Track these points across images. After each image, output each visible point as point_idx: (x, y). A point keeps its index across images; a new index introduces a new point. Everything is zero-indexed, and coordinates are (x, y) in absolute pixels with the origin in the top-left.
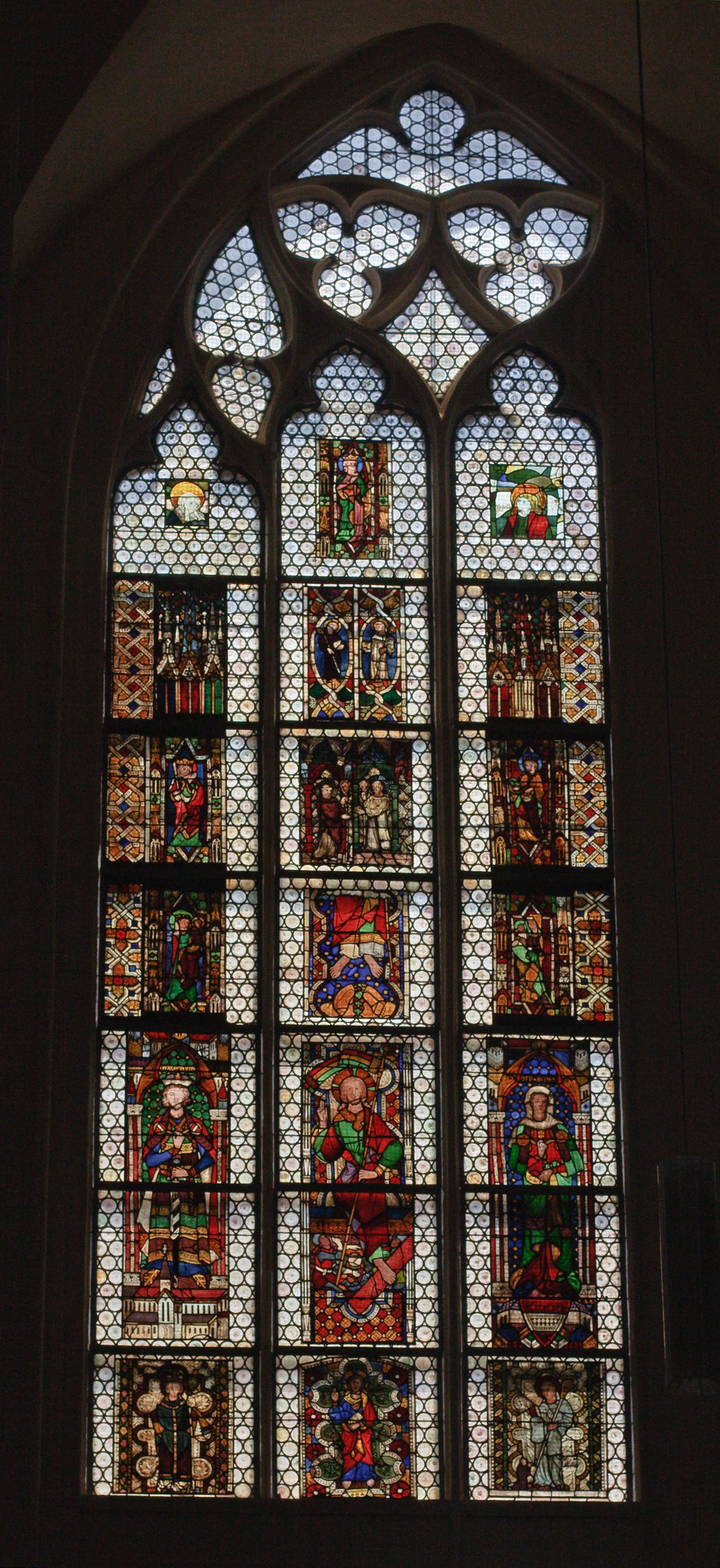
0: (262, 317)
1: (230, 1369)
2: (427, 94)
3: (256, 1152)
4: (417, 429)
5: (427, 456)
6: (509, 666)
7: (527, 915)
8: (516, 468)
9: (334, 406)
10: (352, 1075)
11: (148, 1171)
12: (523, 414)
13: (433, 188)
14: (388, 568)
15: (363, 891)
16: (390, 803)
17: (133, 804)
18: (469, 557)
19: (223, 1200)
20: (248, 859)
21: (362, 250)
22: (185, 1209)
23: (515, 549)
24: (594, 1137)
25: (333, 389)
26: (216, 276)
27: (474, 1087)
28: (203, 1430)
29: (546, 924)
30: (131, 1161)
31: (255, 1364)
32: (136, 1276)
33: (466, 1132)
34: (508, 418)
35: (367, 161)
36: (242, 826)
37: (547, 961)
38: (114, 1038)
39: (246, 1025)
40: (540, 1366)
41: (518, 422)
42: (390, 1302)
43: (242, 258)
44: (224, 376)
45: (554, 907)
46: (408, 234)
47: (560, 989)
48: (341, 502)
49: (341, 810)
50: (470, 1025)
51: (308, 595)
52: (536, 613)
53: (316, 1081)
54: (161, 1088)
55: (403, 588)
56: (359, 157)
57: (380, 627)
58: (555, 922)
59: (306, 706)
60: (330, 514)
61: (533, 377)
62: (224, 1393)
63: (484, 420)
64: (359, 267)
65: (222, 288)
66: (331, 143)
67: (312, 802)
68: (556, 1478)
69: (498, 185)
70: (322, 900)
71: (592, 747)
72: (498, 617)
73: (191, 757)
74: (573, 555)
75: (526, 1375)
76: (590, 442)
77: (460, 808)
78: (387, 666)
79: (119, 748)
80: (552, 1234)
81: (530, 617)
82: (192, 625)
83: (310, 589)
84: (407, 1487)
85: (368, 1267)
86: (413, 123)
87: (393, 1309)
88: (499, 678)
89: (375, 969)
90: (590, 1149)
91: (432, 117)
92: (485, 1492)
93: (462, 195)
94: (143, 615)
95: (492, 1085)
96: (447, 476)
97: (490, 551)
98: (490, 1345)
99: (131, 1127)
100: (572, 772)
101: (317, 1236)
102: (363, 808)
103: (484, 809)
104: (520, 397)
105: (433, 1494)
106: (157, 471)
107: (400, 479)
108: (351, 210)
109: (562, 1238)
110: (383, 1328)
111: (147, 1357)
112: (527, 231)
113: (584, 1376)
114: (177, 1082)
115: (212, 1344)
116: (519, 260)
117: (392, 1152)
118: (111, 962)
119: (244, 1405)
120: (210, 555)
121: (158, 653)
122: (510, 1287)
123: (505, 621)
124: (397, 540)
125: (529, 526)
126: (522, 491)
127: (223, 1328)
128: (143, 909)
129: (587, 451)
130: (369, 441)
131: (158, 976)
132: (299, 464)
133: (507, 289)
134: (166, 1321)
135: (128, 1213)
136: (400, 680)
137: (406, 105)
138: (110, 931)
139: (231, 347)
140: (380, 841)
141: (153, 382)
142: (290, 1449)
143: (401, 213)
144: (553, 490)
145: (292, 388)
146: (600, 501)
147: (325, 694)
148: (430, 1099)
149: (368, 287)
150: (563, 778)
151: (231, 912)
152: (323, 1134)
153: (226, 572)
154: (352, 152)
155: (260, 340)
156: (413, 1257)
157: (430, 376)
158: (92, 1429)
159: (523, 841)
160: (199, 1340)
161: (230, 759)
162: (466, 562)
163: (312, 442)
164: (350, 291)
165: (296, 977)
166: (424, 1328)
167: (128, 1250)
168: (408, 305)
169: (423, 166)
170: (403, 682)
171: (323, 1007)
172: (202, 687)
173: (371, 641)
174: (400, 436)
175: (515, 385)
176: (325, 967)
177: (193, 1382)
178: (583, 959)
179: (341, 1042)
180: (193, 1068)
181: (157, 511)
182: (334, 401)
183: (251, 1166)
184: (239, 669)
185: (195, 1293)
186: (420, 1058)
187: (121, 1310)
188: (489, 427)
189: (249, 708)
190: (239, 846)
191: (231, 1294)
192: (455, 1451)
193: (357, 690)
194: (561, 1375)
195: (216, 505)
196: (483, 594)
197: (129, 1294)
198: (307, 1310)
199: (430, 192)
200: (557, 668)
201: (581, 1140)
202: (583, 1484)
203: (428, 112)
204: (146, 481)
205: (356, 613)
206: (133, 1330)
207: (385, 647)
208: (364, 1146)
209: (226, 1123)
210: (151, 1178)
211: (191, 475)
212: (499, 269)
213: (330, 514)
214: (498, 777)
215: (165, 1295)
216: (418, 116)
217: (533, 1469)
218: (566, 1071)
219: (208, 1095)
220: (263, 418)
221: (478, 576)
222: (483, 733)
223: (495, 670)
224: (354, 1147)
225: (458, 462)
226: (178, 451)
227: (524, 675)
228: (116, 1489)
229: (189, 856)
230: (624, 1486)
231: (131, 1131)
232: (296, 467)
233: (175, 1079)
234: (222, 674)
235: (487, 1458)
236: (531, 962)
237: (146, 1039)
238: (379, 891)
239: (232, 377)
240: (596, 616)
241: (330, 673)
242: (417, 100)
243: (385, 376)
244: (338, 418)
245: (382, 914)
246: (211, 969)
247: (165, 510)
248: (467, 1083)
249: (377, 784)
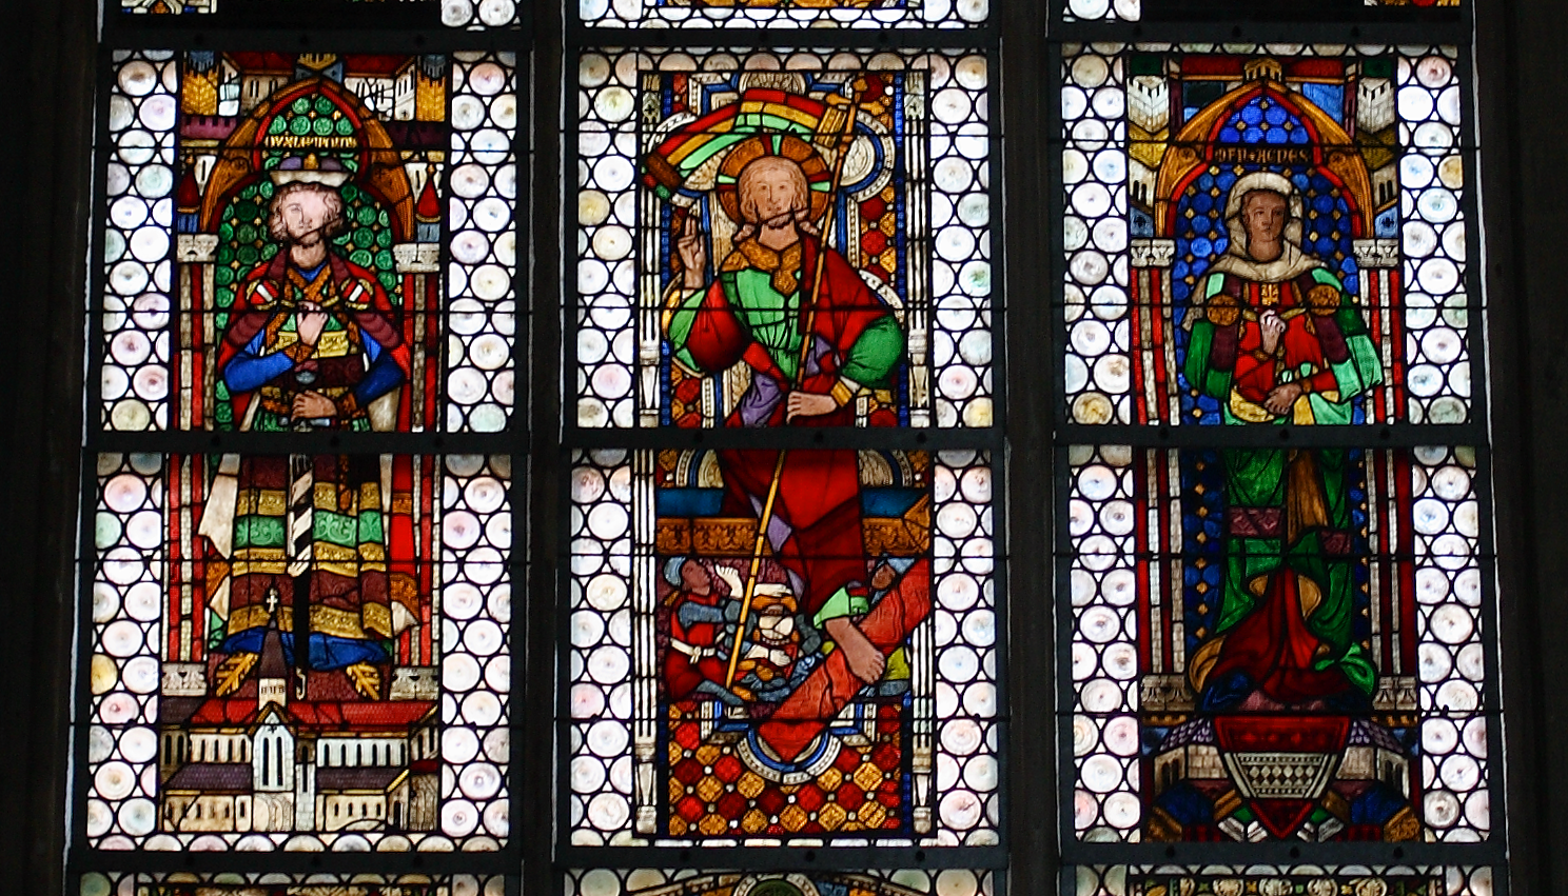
10: (769, 153)
11: (231, 403)
24: (1410, 300)
32: (195, 674)
33: (1071, 292)
42: (870, 728)
50: (1081, 22)
53: (676, 169)
80: (1300, 549)
85: (809, 639)
90: (1400, 331)
95: (1139, 173)
99: (186, 292)
101: (675, 563)
110: (851, 797)
111: (221, 878)
115: (398, 843)
122: (1189, 686)
127: (425, 802)
134: (273, 784)
148: (977, 209)
152: (696, 301)
160: (361, 833)
167: (175, 606)
180: (350, 141)
185: (349, 711)
187: (155, 760)
191: (448, 713)
197: (175, 718)
198: (647, 753)
201: (1375, 306)
206: (185, 810)
208: (801, 331)
210: (238, 419)
215: (273, 718)
219: (390, 207)
224: (776, 335)
231: (186, 303)
233: (302, 168)
248: (1074, 166)
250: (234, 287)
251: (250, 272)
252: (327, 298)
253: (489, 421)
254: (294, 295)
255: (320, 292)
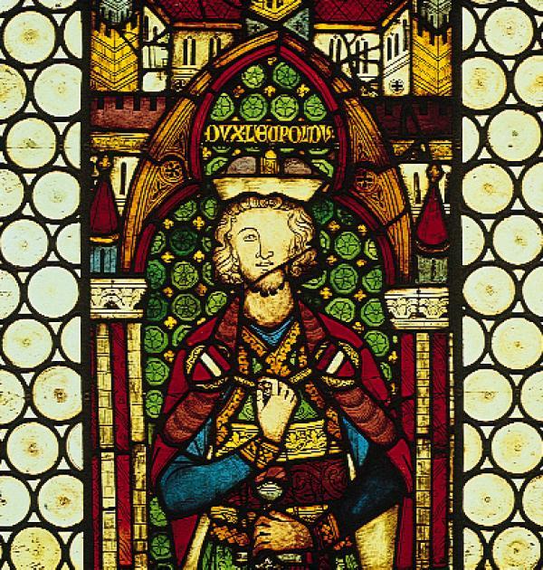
30: (109, 501)
114: (268, 186)
180: (324, 131)
209: (445, 341)
219: (379, 232)
231: (105, 382)
233: (258, 174)
250: (169, 355)
251: (191, 332)
252: (295, 369)
254: (250, 368)
255: (286, 363)
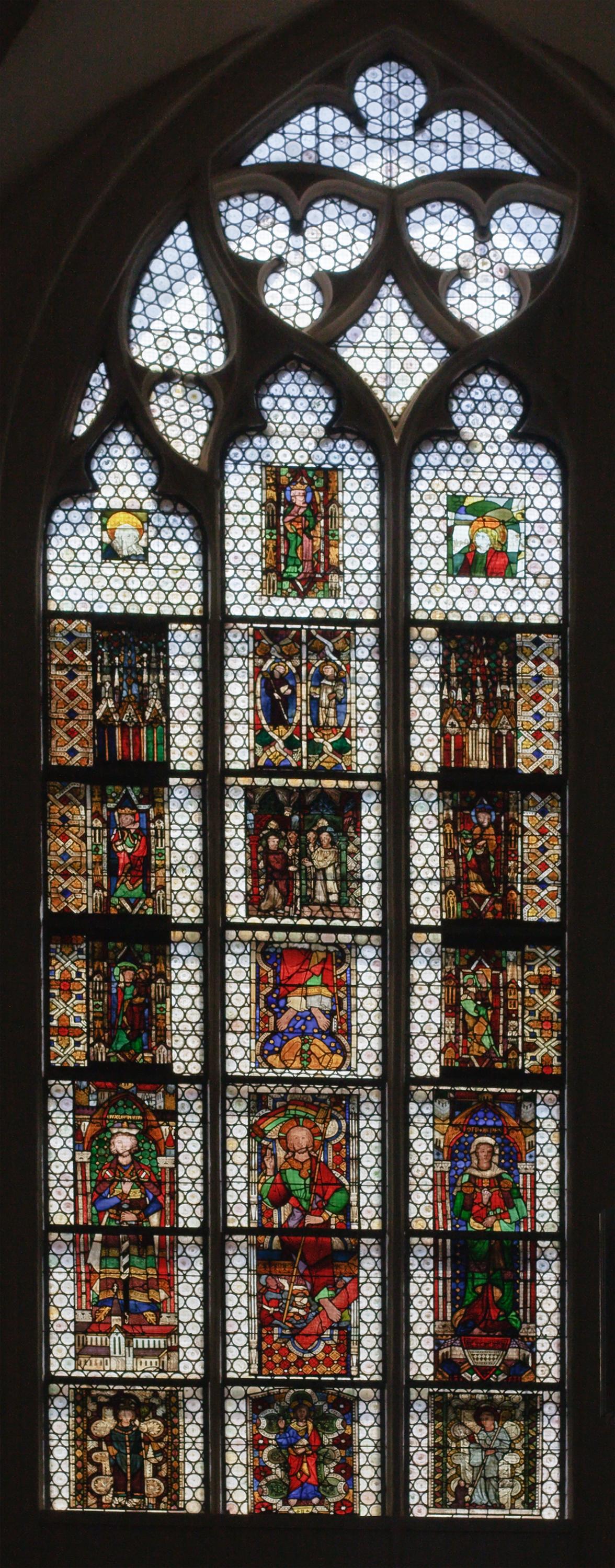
0: (203, 327)
1: (181, 1398)
2: (386, 65)
3: (204, 1198)
4: (370, 455)
5: (381, 485)
6: (464, 713)
7: (477, 969)
8: (476, 500)
9: (281, 429)
10: (298, 1125)
12: (485, 439)
13: (390, 179)
14: (338, 607)
15: (310, 944)
16: (338, 855)
17: (75, 854)
18: (424, 597)
19: (172, 1243)
20: (193, 911)
21: (312, 251)
22: (135, 1251)
23: (473, 588)
24: (538, 1186)
25: (279, 410)
26: (152, 280)
27: (420, 1137)
28: (155, 1452)
29: (495, 978)
30: (81, 1206)
31: (205, 1394)
32: (87, 1313)
33: (412, 1180)
34: (468, 443)
35: (317, 146)
36: (186, 877)
37: (496, 1015)
38: (60, 1088)
39: (192, 1075)
40: (480, 1397)
41: (478, 448)
42: (335, 1338)
43: (180, 259)
44: (162, 394)
45: (504, 961)
46: (362, 232)
47: (508, 1043)
48: (289, 535)
49: (287, 862)
50: (417, 1077)
51: (253, 636)
52: (493, 657)
53: (263, 1130)
54: (109, 1135)
55: (353, 630)
56: (309, 141)
57: (329, 671)
58: (505, 976)
59: (252, 754)
60: (277, 548)
61: (496, 398)
62: (175, 1420)
63: (442, 446)
64: (309, 271)
65: (159, 293)
66: (278, 124)
67: (258, 853)
68: (492, 1498)
69: (463, 176)
70: (269, 953)
71: (548, 798)
72: (453, 661)
73: (133, 807)
74: (534, 595)
75: (466, 1405)
76: (555, 472)
77: (411, 860)
78: (336, 712)
79: (58, 796)
81: (486, 661)
82: (132, 667)
83: (256, 629)
84: (351, 1505)
85: (314, 1306)
86: (370, 101)
87: (338, 1345)
88: (453, 726)
89: (323, 1022)
90: (534, 1197)
91: (391, 93)
92: (424, 1510)
93: (423, 187)
94: (81, 656)
96: (401, 508)
97: (446, 590)
98: (432, 1379)
99: (79, 1173)
100: (526, 824)
101: (264, 1277)
102: (311, 860)
103: (435, 862)
104: (481, 420)
105: (375, 1511)
106: (92, 500)
107: (351, 511)
108: (300, 204)
109: (504, 1280)
110: (329, 1363)
112: (493, 230)
113: (522, 1407)
114: (125, 1130)
115: (163, 1376)
116: (484, 264)
117: (338, 1199)
118: (55, 1013)
119: (194, 1431)
120: (150, 592)
121: (97, 696)
122: (452, 1326)
123: (461, 666)
124: (348, 578)
125: (488, 564)
126: (481, 525)
127: (173, 1361)
128: (87, 960)
129: (552, 481)
130: (319, 468)
131: (104, 1026)
132: (244, 493)
133: (470, 297)
135: (78, 1254)
136: (349, 727)
137: (362, 79)
138: (53, 983)
139: (169, 361)
140: (328, 894)
141: (86, 400)
142: (239, 1471)
143: (355, 208)
144: (514, 523)
145: (237, 410)
146: (564, 537)
147: (272, 742)
148: (376, 1148)
149: (318, 293)
150: (516, 830)
151: (176, 964)
152: (270, 1181)
153: (167, 611)
154: (301, 134)
155: (200, 353)
156: (358, 1297)
157: (385, 395)
158: (48, 1452)
159: (474, 895)
161: (173, 808)
162: (420, 602)
163: (257, 469)
164: (298, 298)
165: (242, 1028)
166: (368, 1361)
167: (79, 1289)
168: (362, 315)
169: (380, 152)
170: (353, 730)
171: (270, 1059)
172: (144, 733)
173: (320, 686)
174: (352, 463)
175: (476, 406)
176: (272, 1020)
177: (145, 1410)
178: (532, 1013)
179: (287, 1093)
180: (140, 1117)
181: (93, 544)
182: (281, 423)
183: (199, 1211)
184: (181, 715)
185: (145, 1328)
186: (367, 1109)
187: (74, 1344)
188: (447, 453)
189: (192, 755)
190: (184, 898)
191: (181, 1330)
192: (396, 1473)
193: (305, 737)
194: (500, 1406)
195: (155, 538)
196: (438, 636)
197: (81, 1330)
198: (254, 1345)
199: (387, 183)
200: (513, 715)
201: (525, 1188)
202: (518, 1503)
203: (387, 89)
204: (81, 511)
205: (304, 656)
207: (334, 692)
209: (173, 1171)
210: (100, 1221)
211: (129, 505)
212: (461, 273)
213: (277, 548)
214: (449, 829)
216: (375, 92)
217: (471, 1489)
218: (512, 1122)
219: (156, 1143)
220: (205, 442)
221: (433, 617)
222: (435, 783)
223: (448, 718)
224: (300, 1194)
225: (413, 493)
226: (115, 478)
227: (478, 723)
228: (73, 1505)
229: (133, 907)
230: (557, 1505)
231: (79, 1177)
232: (240, 496)
234: (164, 720)
235: (427, 1480)
236: (480, 1016)
237: (93, 1089)
238: (327, 945)
239: (171, 395)
240: (556, 661)
241: (276, 719)
242: (374, 73)
243: (337, 396)
244: (285, 442)
245: (330, 967)
246: (157, 1020)
247: (101, 543)
248: (413, 1133)
249: (325, 836)
253: (194, 1223)
